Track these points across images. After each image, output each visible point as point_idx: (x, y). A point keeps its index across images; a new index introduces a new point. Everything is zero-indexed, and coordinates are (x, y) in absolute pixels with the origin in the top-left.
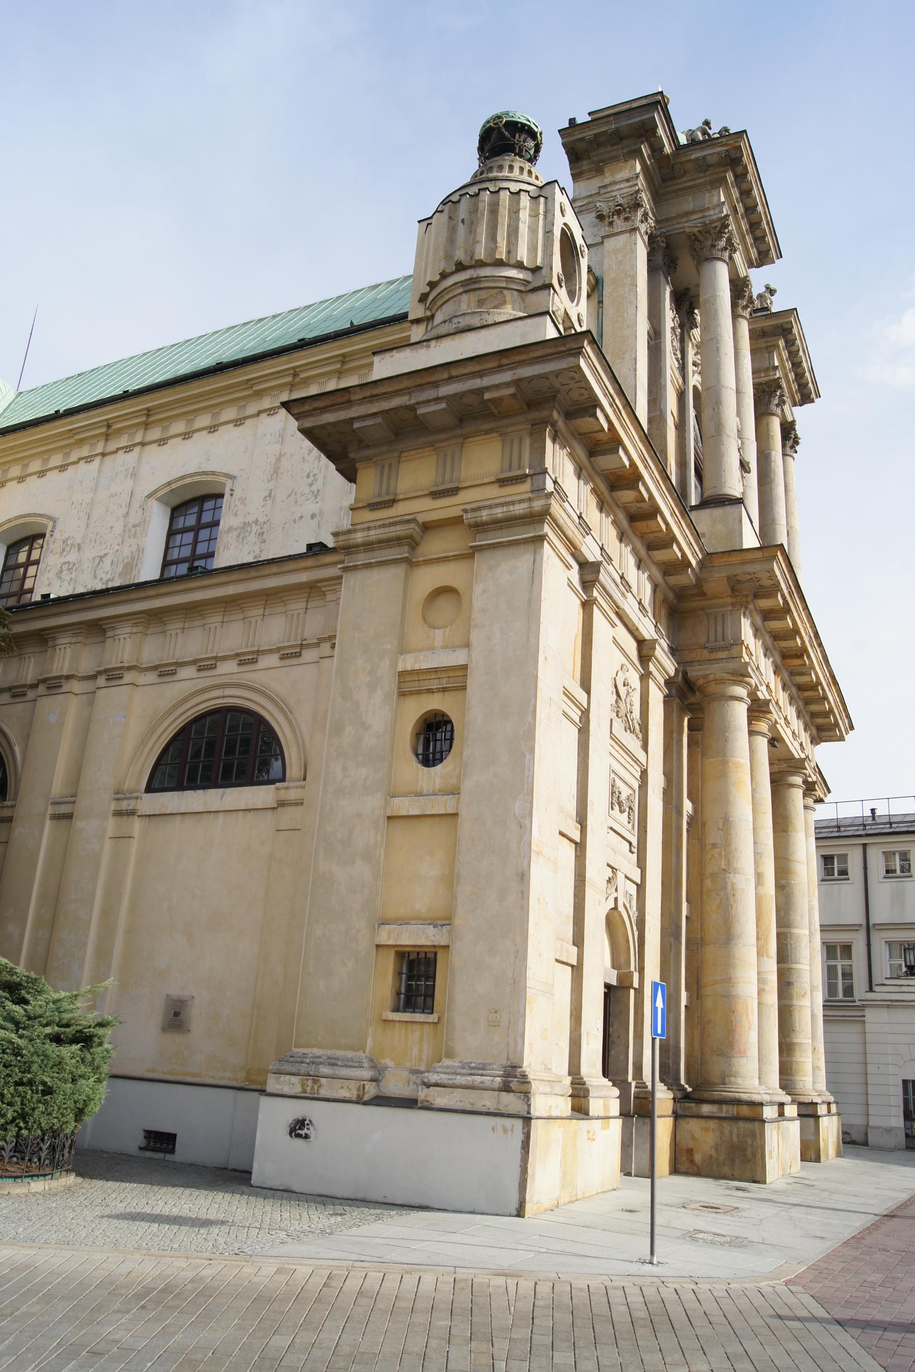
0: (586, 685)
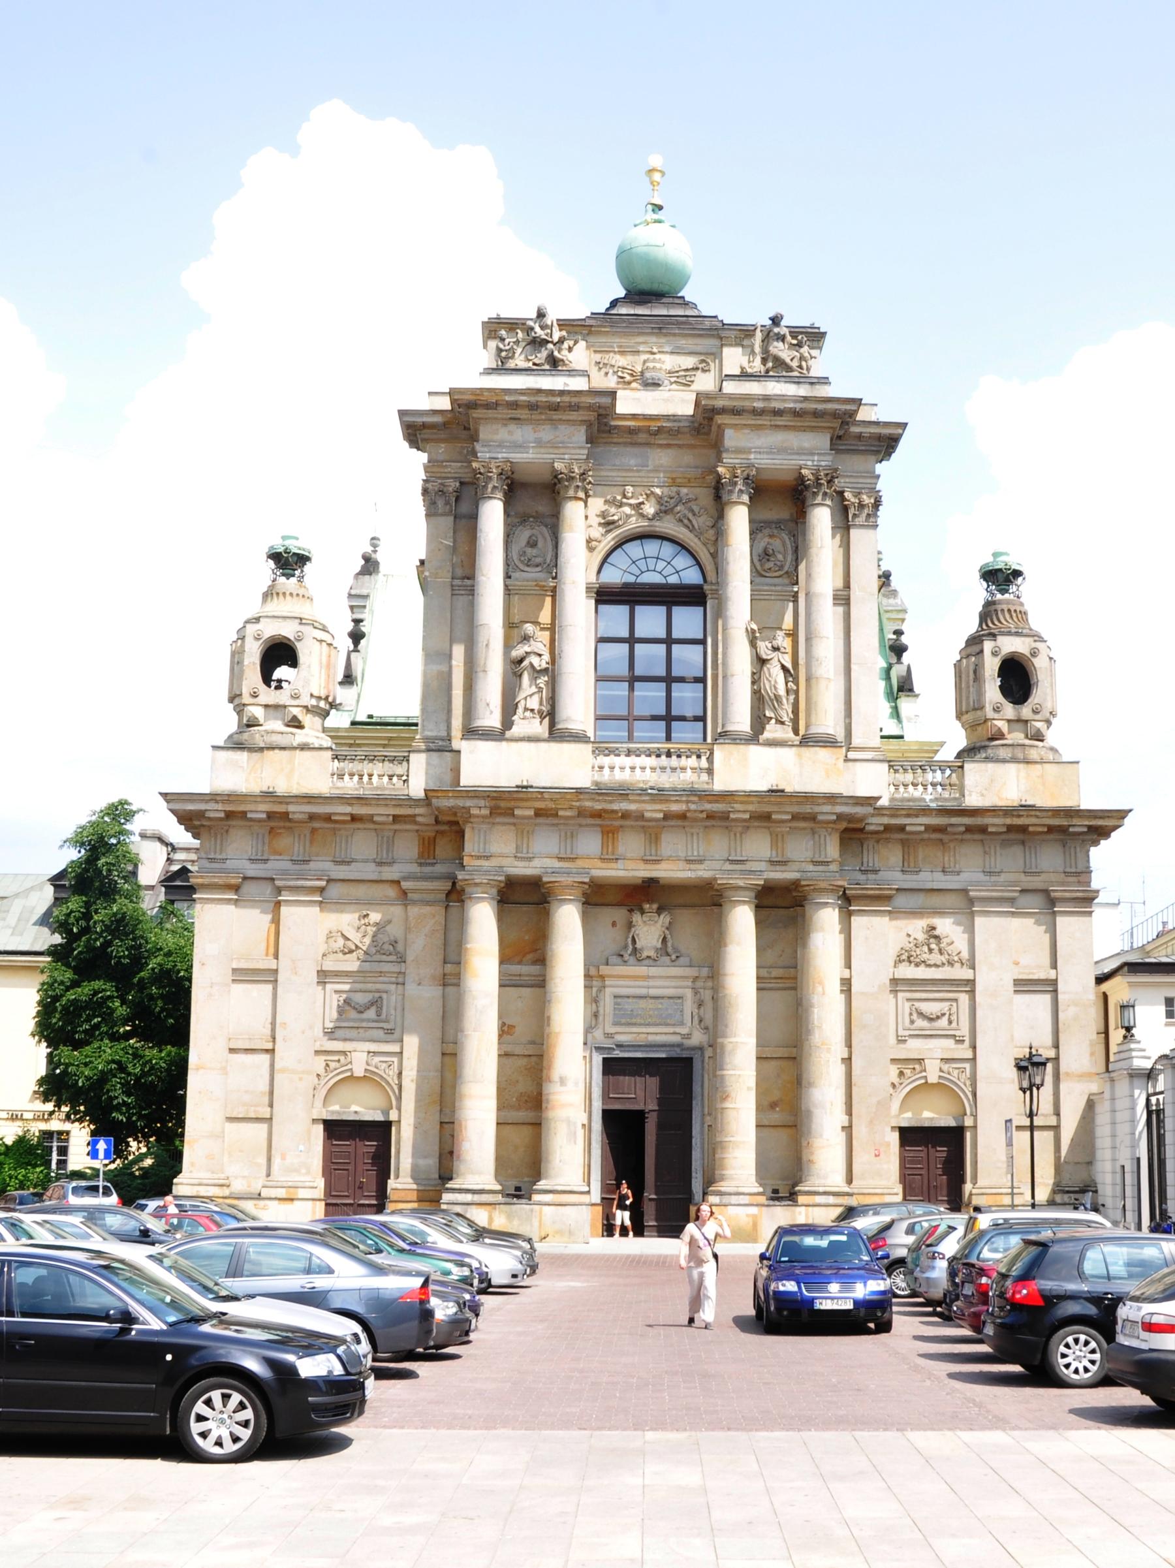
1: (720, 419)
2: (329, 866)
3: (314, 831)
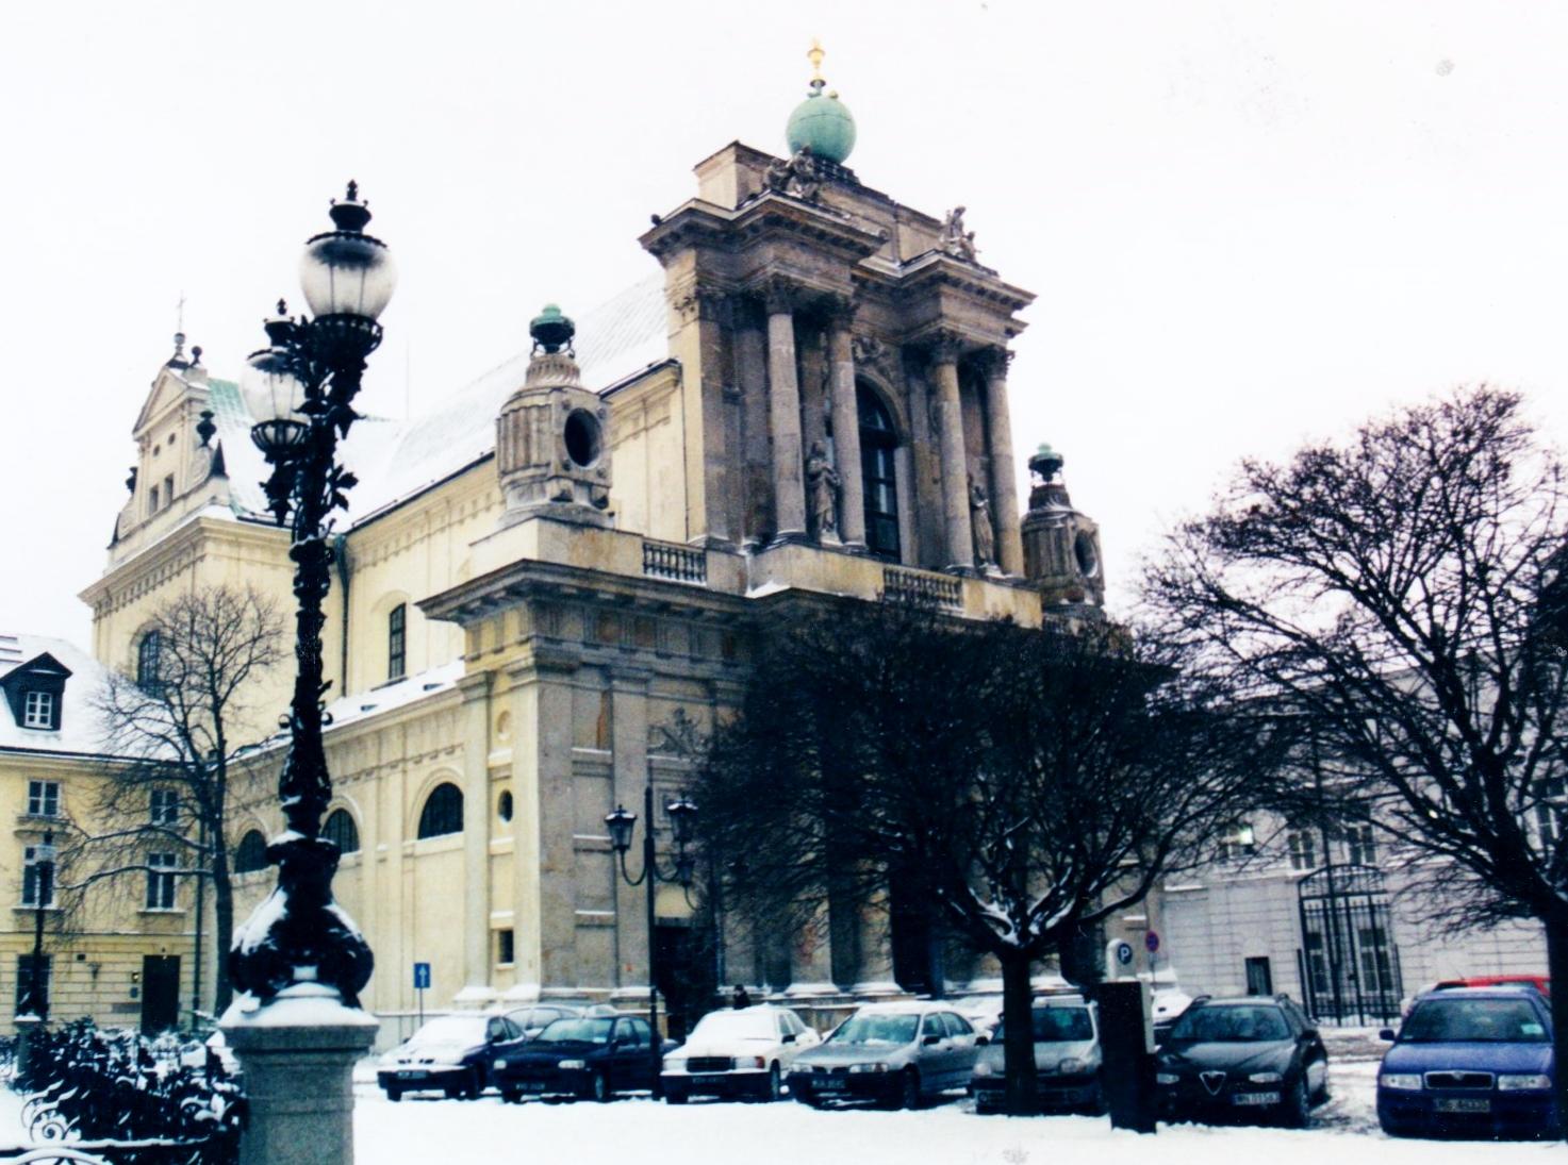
1: (945, 288)
2: (652, 658)
3: (638, 619)
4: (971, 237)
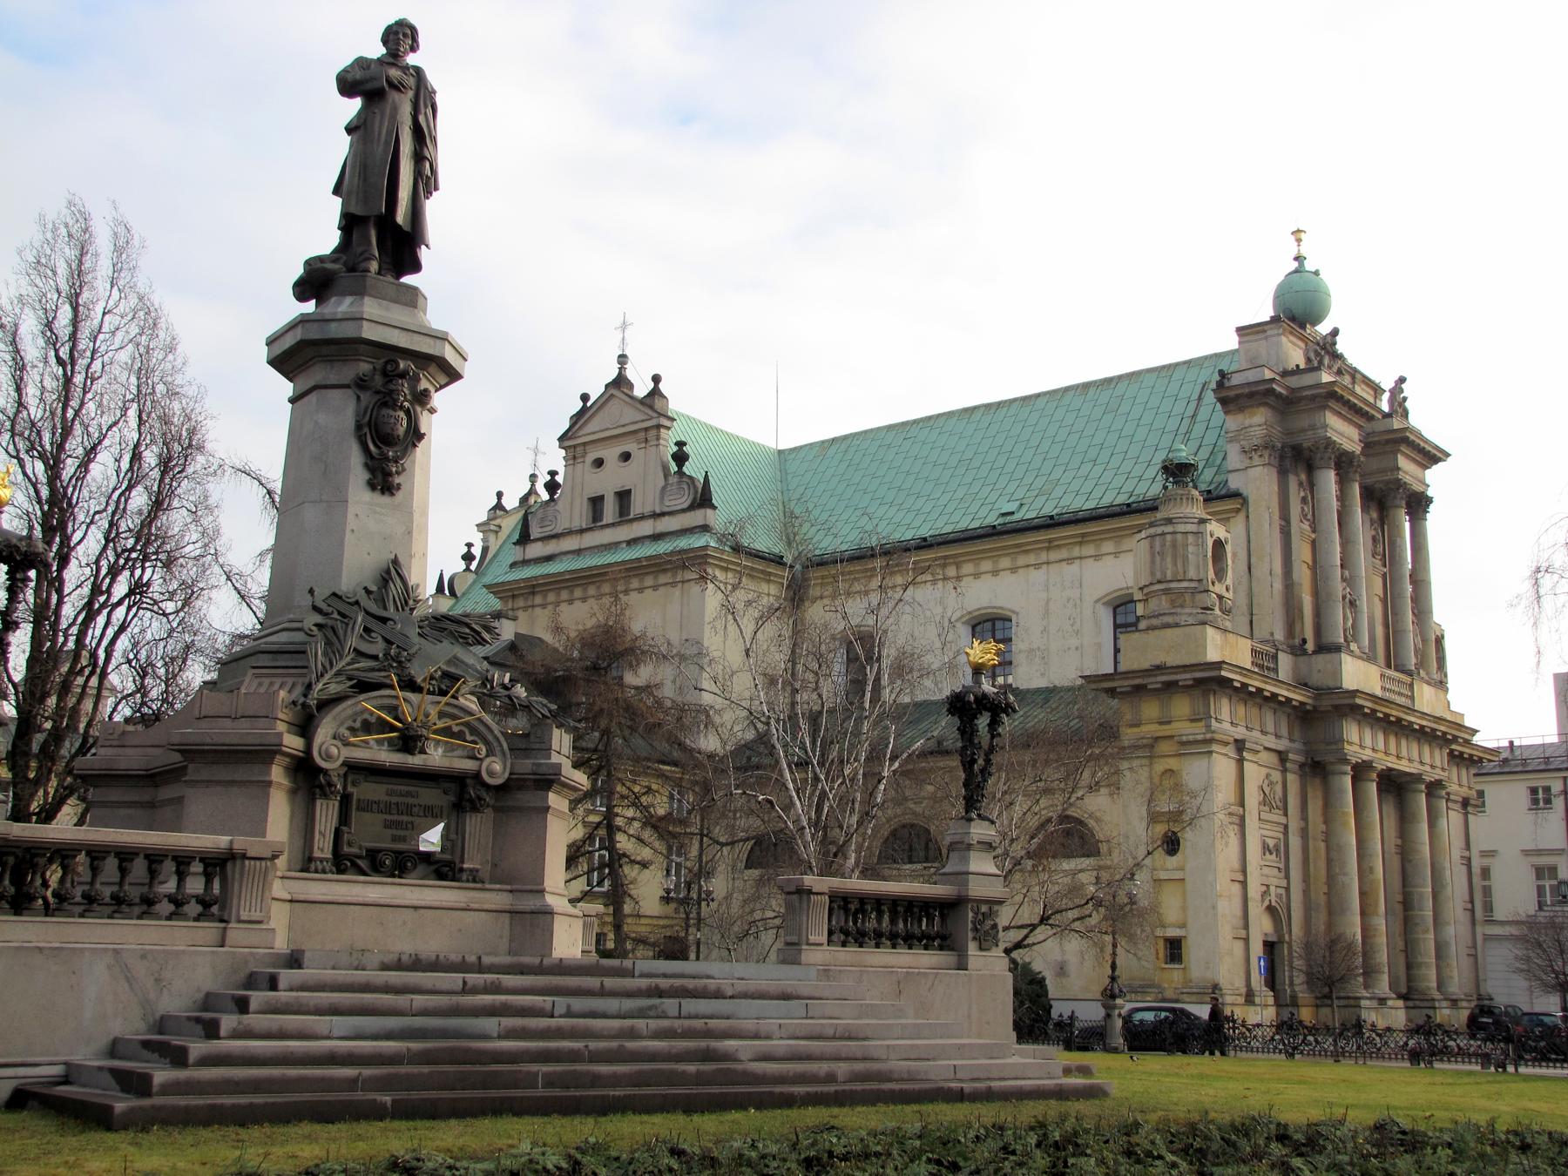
0: (1242, 804)
4: (1405, 399)
